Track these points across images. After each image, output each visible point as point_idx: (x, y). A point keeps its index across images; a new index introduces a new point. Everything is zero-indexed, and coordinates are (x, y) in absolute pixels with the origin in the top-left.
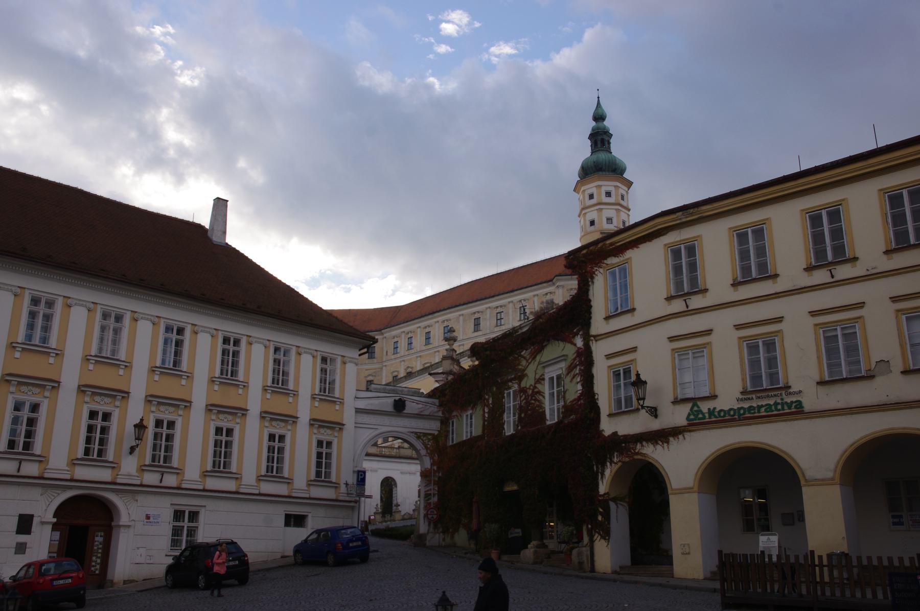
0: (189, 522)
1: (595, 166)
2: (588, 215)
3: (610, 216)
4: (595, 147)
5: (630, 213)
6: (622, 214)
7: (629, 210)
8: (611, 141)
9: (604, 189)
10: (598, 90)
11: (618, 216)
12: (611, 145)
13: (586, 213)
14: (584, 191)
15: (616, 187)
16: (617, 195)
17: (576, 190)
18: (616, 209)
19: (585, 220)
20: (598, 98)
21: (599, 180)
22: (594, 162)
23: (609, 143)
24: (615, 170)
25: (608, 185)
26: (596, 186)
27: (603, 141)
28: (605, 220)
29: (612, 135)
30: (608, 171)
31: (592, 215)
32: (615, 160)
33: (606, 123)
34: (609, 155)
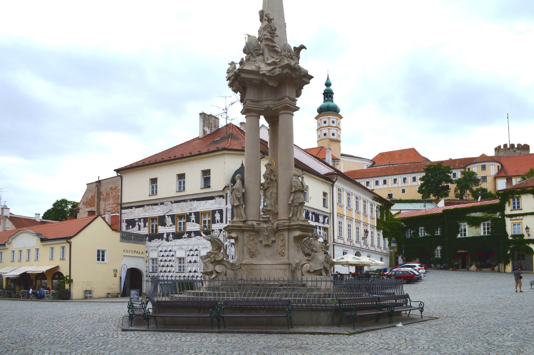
2: (323, 131)
3: (333, 132)
5: (341, 131)
6: (338, 131)
7: (341, 130)
9: (331, 120)
11: (337, 133)
12: (333, 98)
13: (322, 130)
14: (321, 120)
16: (337, 123)
17: (317, 118)
19: (321, 133)
23: (333, 98)
25: (333, 118)
28: (331, 134)
31: (325, 131)
34: (332, 103)
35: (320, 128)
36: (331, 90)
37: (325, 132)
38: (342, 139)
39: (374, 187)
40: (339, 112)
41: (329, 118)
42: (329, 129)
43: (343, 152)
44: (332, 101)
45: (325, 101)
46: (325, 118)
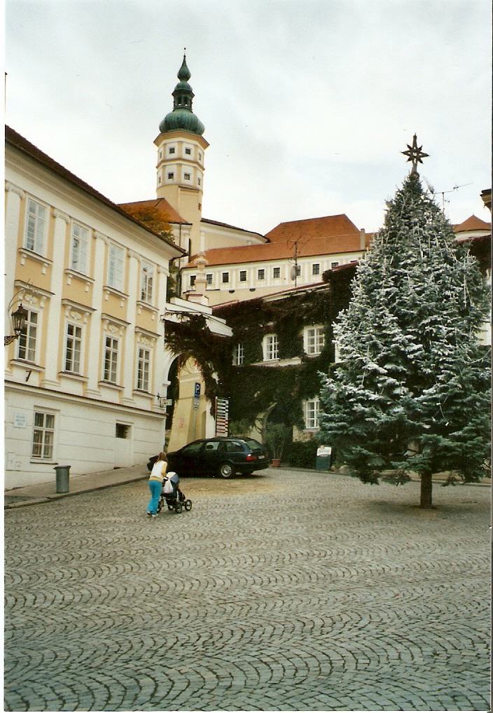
0: (47, 427)
2: (167, 168)
3: (188, 172)
5: (204, 172)
9: (185, 146)
11: (195, 174)
12: (193, 105)
14: (165, 144)
15: (196, 146)
16: (196, 154)
17: (157, 142)
18: (194, 167)
23: (191, 103)
24: (194, 128)
25: (189, 143)
26: (178, 142)
30: (190, 129)
31: (172, 168)
33: (189, 82)
34: (190, 113)
35: (163, 161)
36: (189, 87)
37: (171, 171)
38: (206, 187)
39: (255, 284)
40: (202, 131)
43: (205, 215)
44: (190, 109)
45: (176, 108)
46: (173, 142)
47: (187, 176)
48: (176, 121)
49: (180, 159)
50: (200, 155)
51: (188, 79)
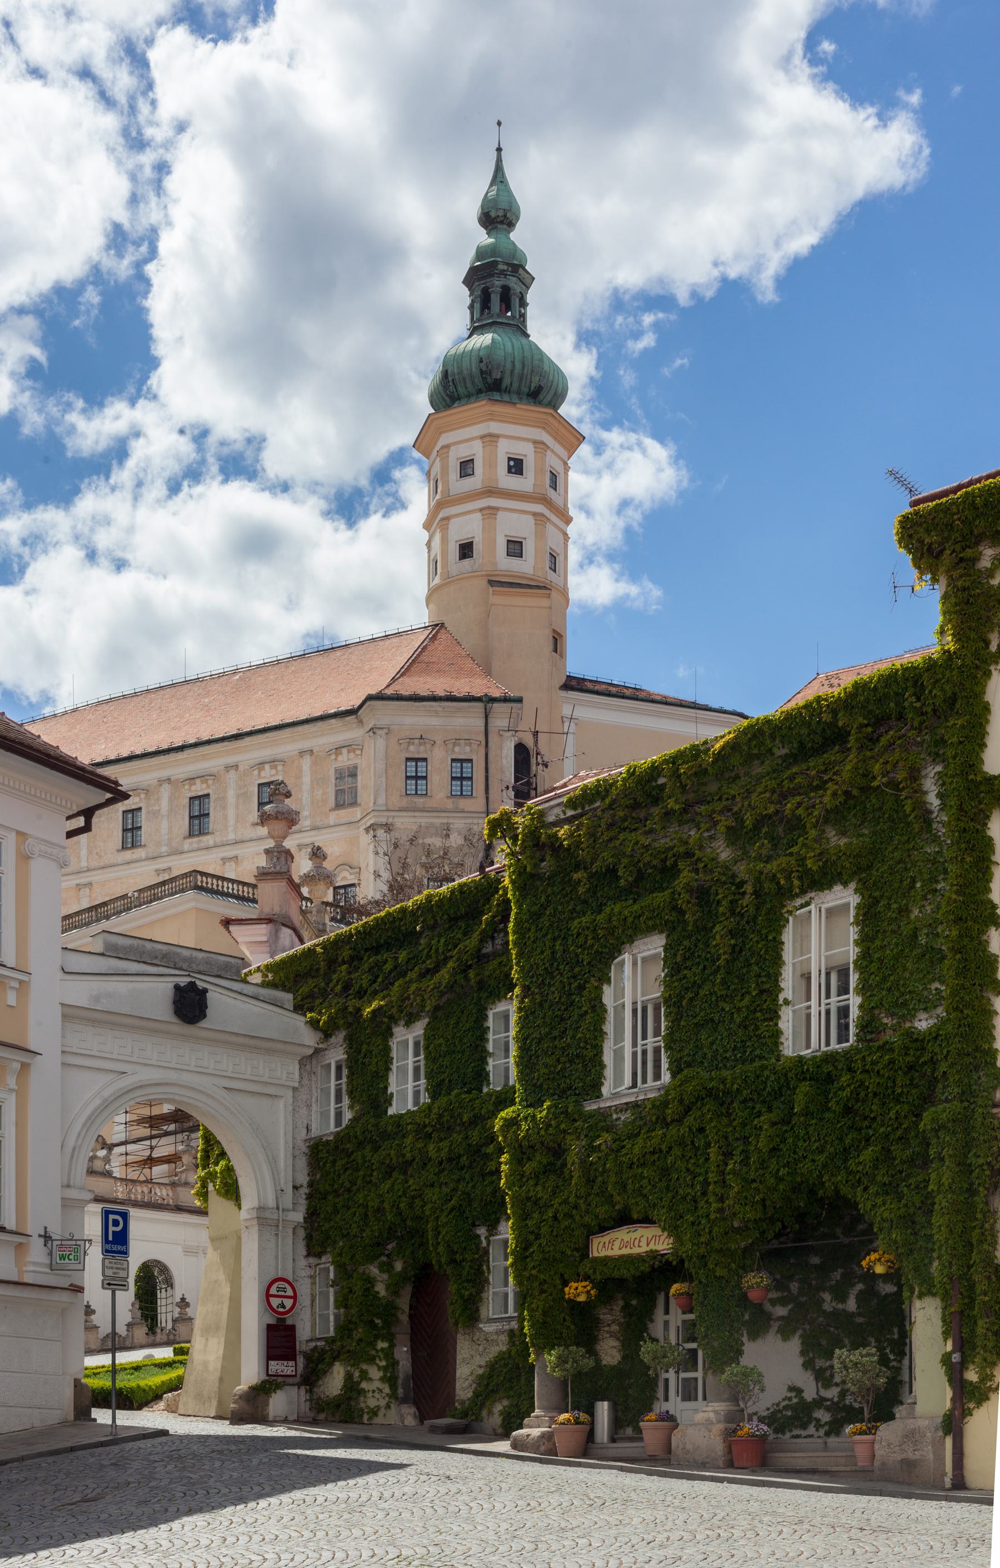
1: (482, 372)
2: (454, 523)
3: (516, 534)
4: (482, 313)
6: (550, 529)
8: (530, 297)
9: (505, 449)
10: (499, 124)
13: (447, 519)
16: (539, 471)
19: (444, 540)
20: (499, 150)
21: (492, 417)
22: (481, 361)
23: (523, 304)
26: (482, 437)
27: (506, 298)
29: (533, 279)
32: (541, 360)
41: (489, 439)
42: (490, 512)
47: (515, 548)
48: (475, 370)
49: (491, 491)
50: (554, 477)
51: (511, 225)
